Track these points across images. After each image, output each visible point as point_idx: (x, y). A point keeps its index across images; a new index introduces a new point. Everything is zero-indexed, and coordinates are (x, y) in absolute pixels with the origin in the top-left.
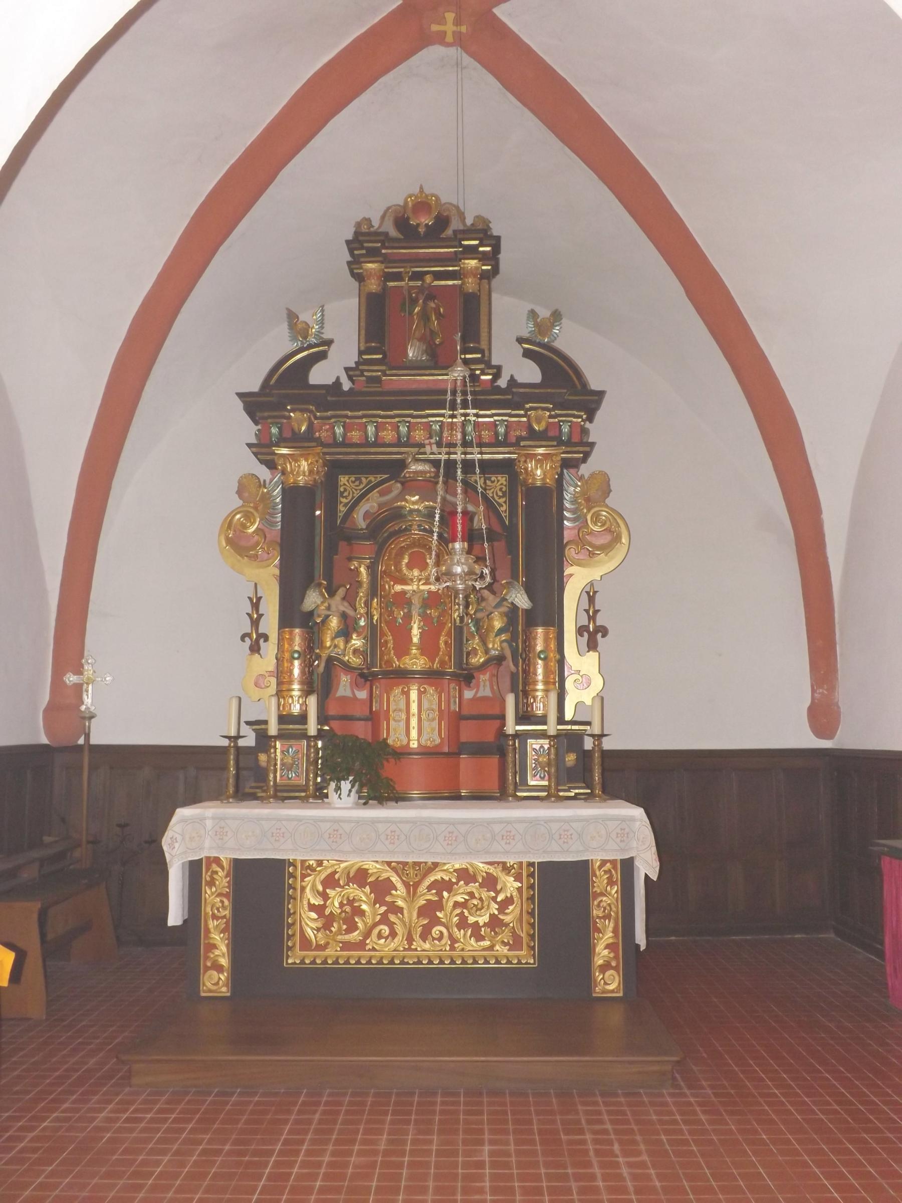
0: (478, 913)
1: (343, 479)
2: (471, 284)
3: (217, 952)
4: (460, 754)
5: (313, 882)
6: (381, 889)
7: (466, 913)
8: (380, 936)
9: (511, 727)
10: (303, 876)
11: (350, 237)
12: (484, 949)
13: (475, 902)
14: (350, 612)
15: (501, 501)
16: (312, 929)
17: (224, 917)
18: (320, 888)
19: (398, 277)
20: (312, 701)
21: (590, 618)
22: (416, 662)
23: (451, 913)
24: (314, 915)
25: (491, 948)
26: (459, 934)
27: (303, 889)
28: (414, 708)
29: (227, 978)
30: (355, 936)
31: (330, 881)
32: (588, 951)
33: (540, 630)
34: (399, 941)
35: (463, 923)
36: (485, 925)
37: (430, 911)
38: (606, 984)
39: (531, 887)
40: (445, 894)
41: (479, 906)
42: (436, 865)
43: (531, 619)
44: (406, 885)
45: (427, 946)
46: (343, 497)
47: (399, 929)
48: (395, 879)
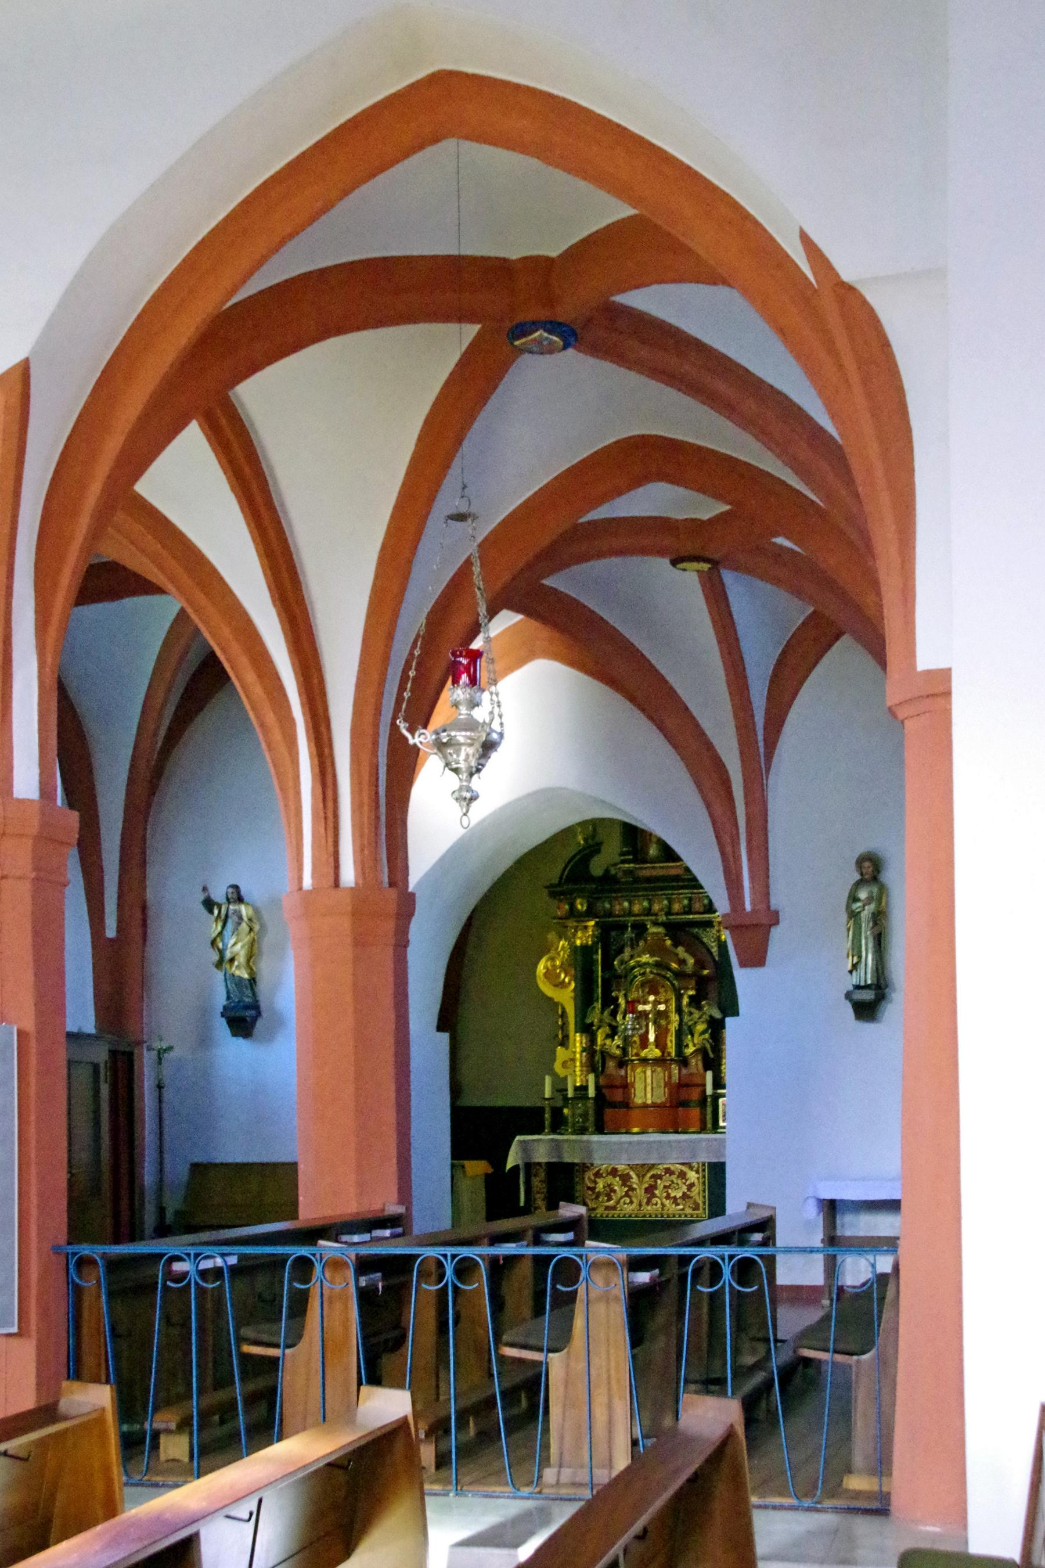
5: (590, 1174)
6: (625, 1179)
9: (709, 1090)
10: (584, 1172)
14: (614, 1024)
15: (713, 944)
18: (593, 1178)
20: (591, 1078)
24: (590, 1192)
25: (683, 1209)
26: (667, 1202)
27: (583, 1178)
28: (649, 1080)
30: (612, 1203)
31: (598, 1174)
35: (668, 1197)
37: (650, 1190)
39: (704, 1177)
42: (653, 1165)
44: (638, 1176)
45: (649, 1208)
47: (634, 1200)
48: (632, 1173)
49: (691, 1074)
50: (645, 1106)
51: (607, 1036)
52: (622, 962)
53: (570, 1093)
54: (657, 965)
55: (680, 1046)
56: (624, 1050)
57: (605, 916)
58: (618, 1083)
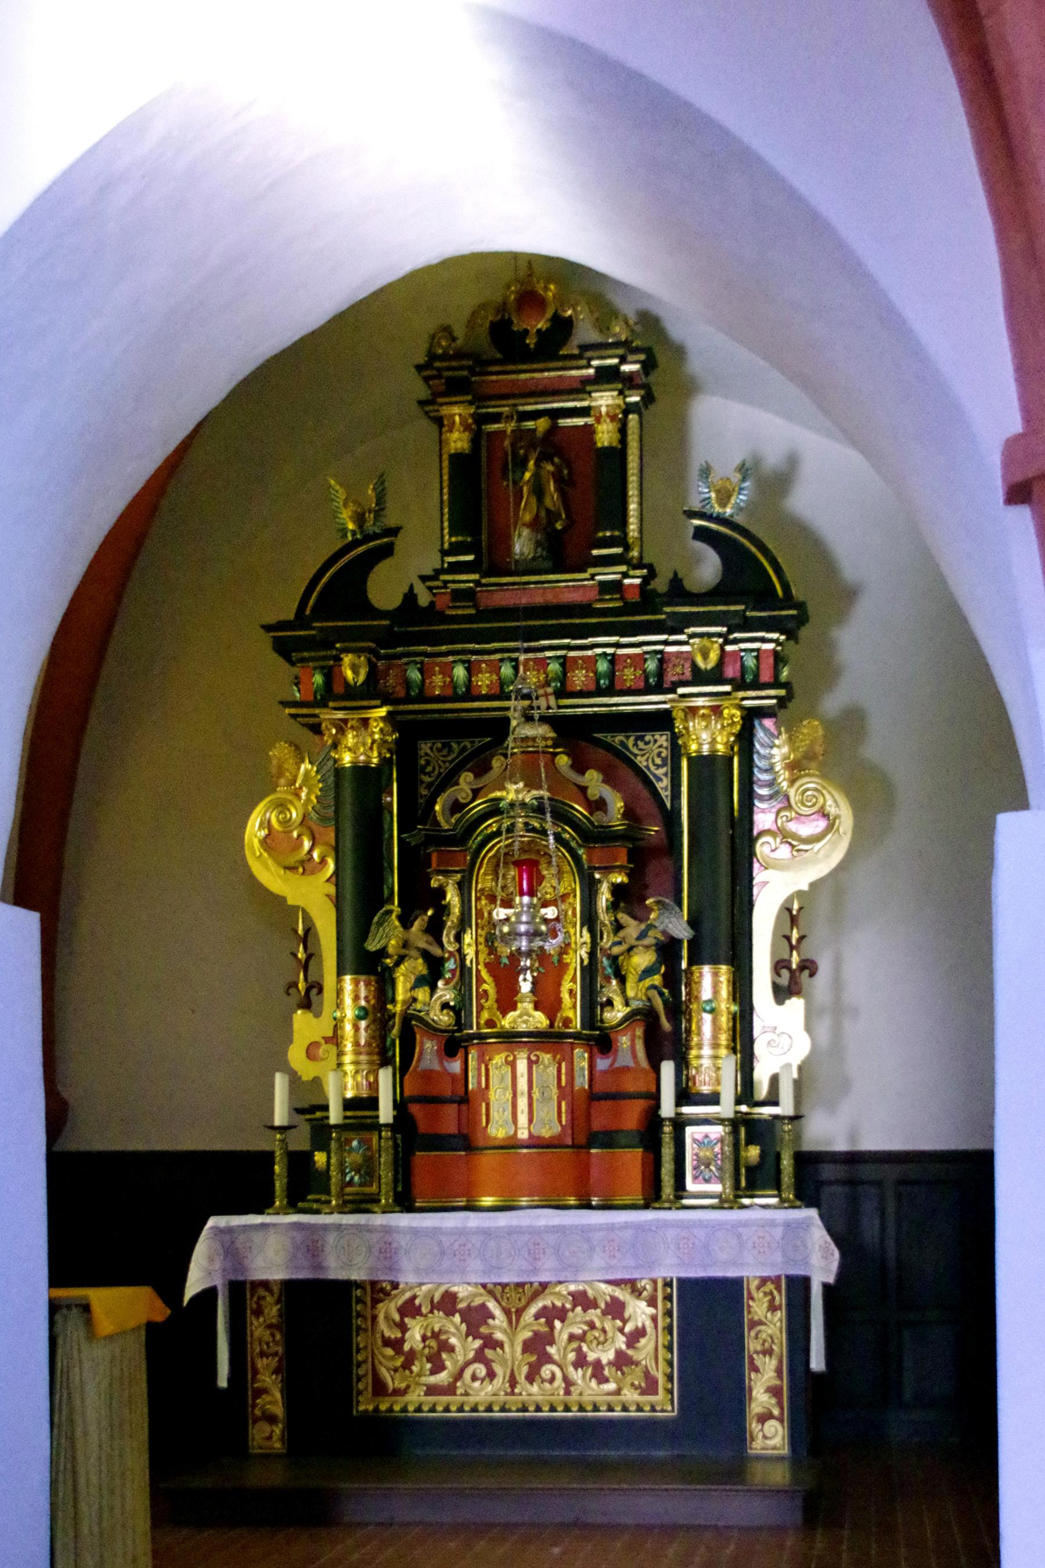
1: (425, 747)
46: (426, 774)
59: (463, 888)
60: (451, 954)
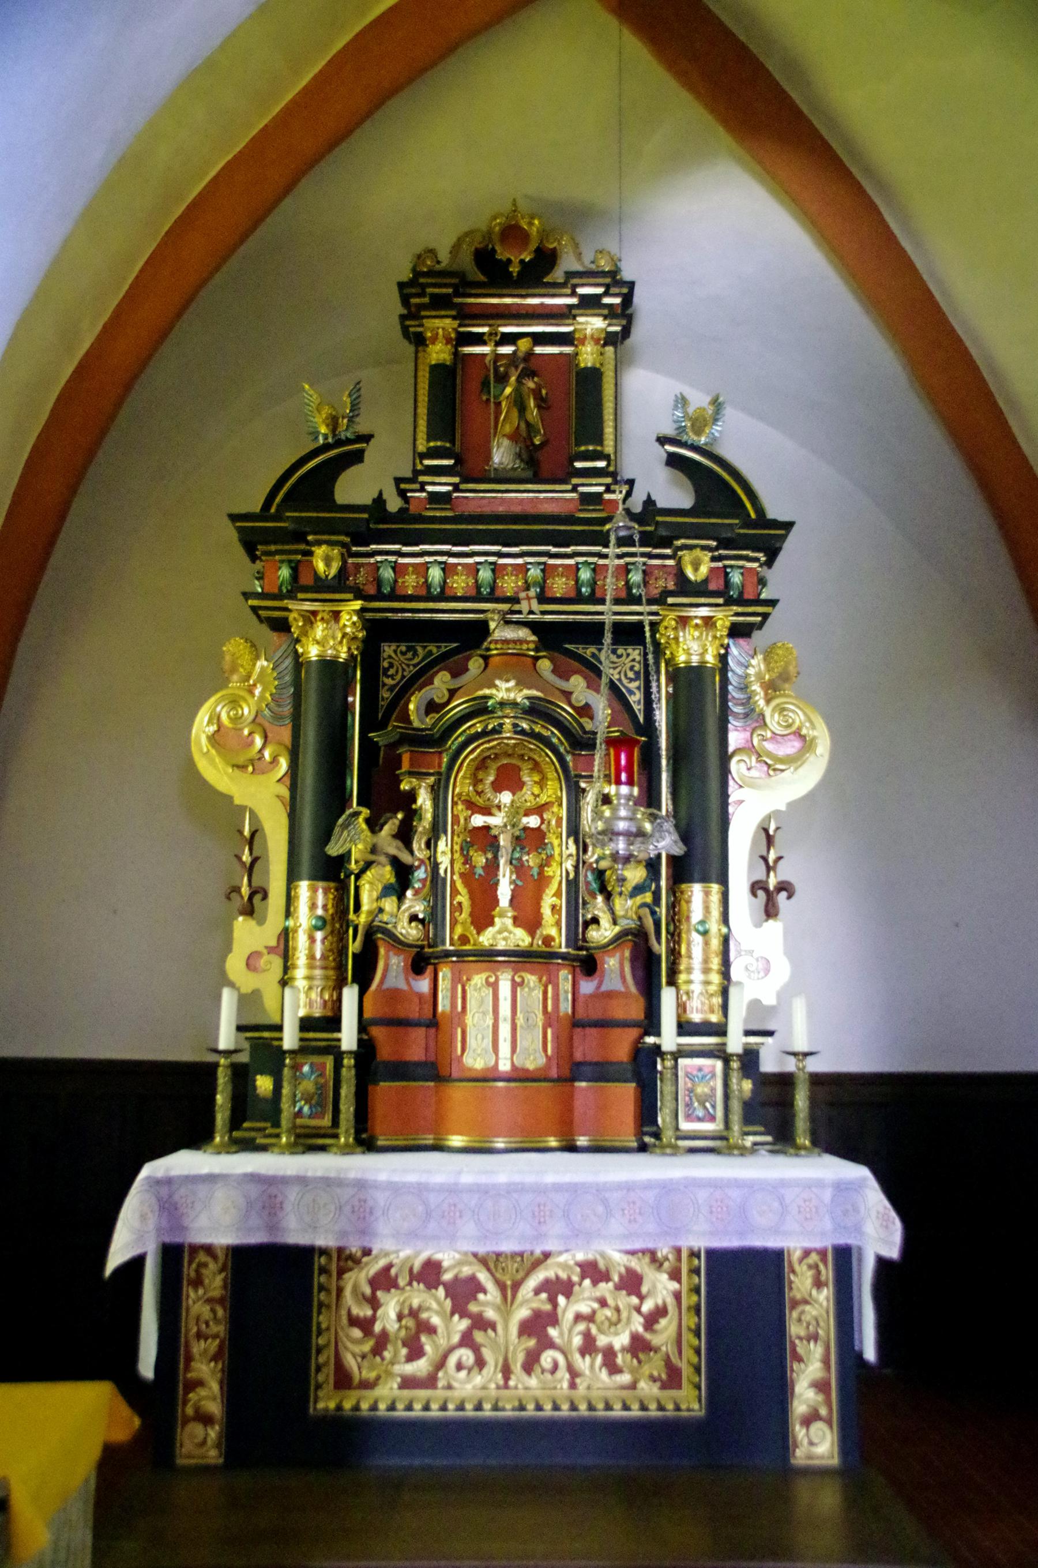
0: (612, 1329)
1: (388, 650)
2: (588, 356)
3: (202, 1392)
4: (573, 1079)
5: (359, 1279)
7: (594, 1330)
8: (459, 1367)
10: (341, 1272)
11: (406, 275)
12: (623, 1388)
13: (608, 1312)
14: (405, 858)
15: (633, 685)
16: (354, 1356)
17: (215, 1336)
18: (368, 1291)
19: (479, 339)
21: (769, 869)
22: (504, 933)
23: (570, 1331)
24: (357, 1333)
25: (633, 1386)
26: (583, 1364)
27: (340, 1291)
29: (220, 1436)
30: (420, 1367)
31: (384, 1280)
32: (783, 1390)
33: (696, 890)
34: (491, 1374)
36: (624, 1349)
37: (537, 1326)
38: (811, 1443)
40: (561, 1300)
41: (614, 1318)
42: (547, 1255)
43: (683, 870)
44: (502, 1287)
45: (533, 1382)
46: (388, 677)
47: (487, 1353)
48: (483, 1276)
49: (610, 995)
50: (489, 1076)
51: (386, 891)
52: (432, 707)
53: (289, 1040)
54: (536, 710)
55: (579, 926)
56: (432, 921)
57: (380, 597)
58: (413, 1011)
59: (438, 793)
60: (422, 862)
